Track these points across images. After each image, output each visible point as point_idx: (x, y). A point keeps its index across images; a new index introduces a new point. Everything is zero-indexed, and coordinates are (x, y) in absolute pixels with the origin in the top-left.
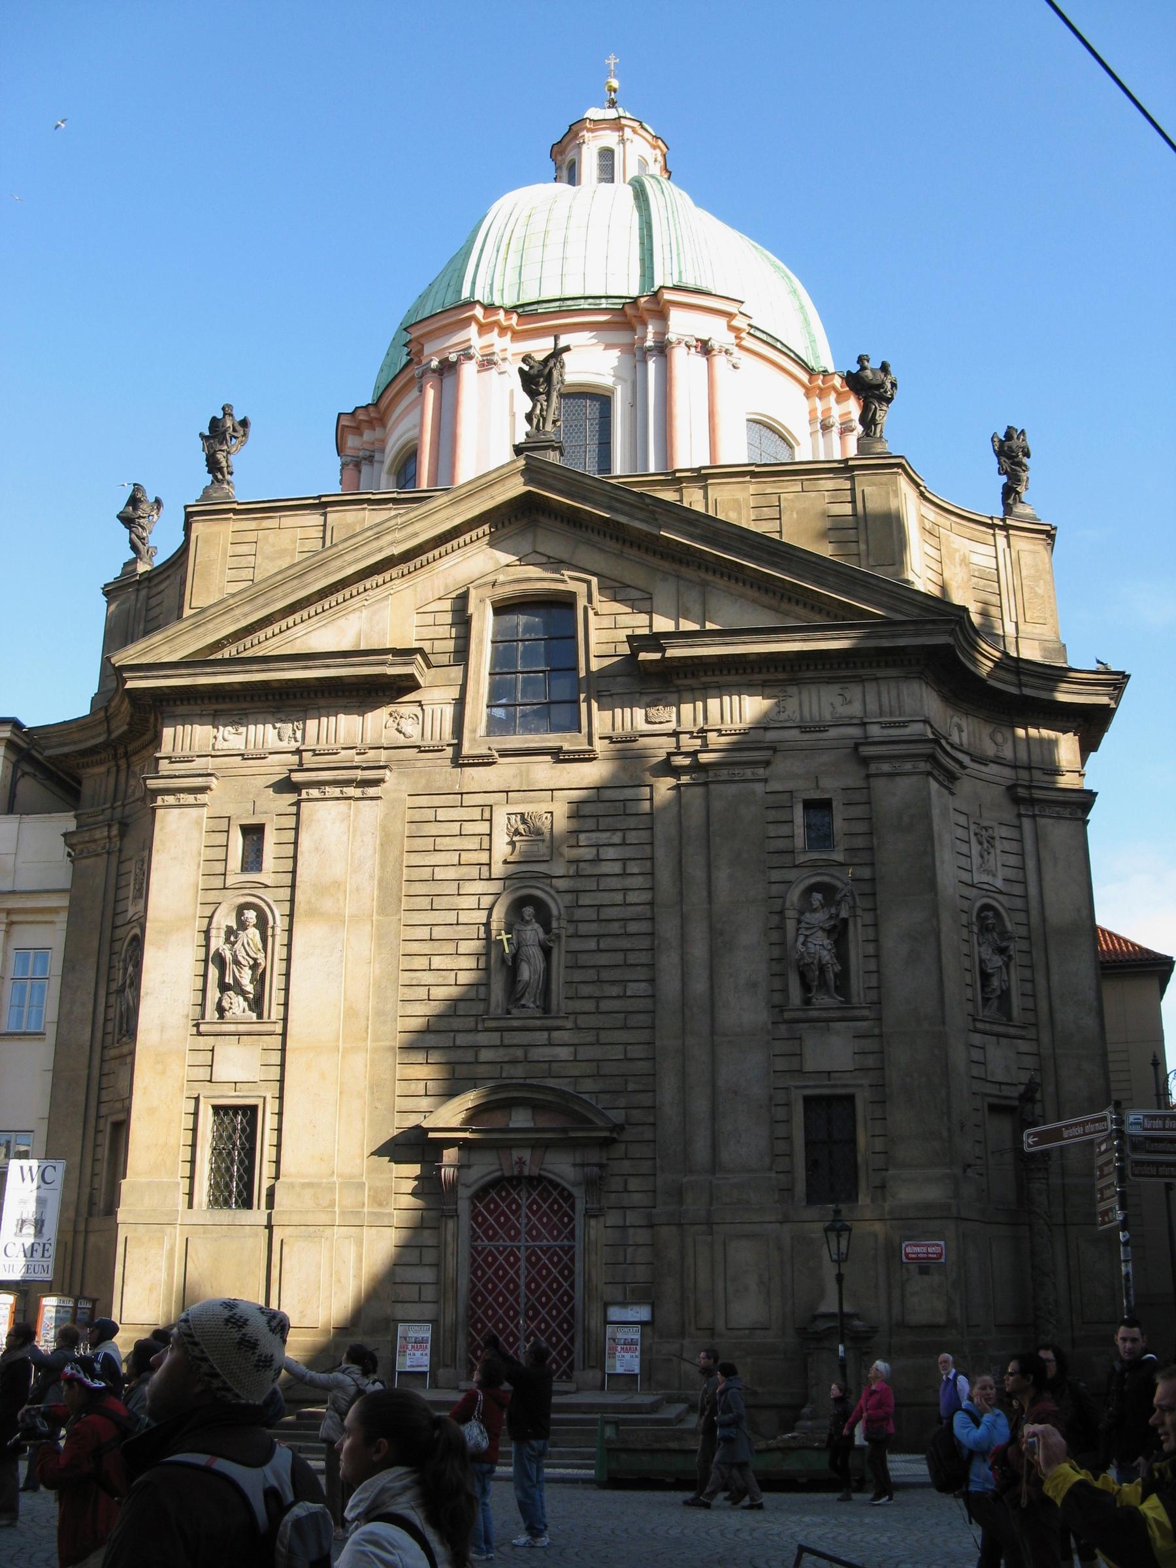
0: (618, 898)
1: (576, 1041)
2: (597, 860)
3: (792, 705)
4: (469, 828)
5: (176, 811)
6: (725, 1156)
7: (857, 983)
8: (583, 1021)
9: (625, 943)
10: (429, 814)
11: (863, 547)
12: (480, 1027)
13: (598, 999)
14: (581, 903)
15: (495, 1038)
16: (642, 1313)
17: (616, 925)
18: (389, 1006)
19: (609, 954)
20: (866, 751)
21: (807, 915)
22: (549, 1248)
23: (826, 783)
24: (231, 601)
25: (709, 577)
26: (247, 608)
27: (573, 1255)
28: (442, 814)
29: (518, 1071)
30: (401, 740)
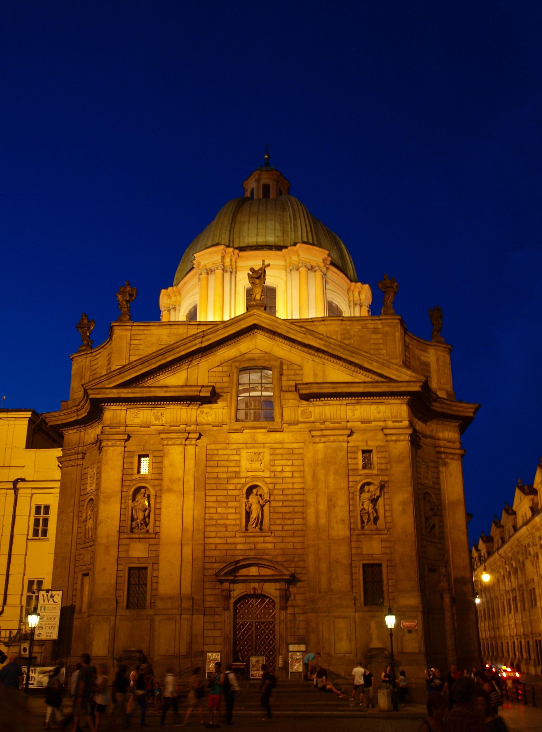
0: (291, 486)
1: (275, 541)
2: (282, 471)
3: (357, 413)
4: (232, 458)
5: (112, 448)
6: (333, 586)
7: (381, 521)
8: (277, 533)
9: (294, 504)
10: (215, 452)
11: (385, 351)
14: (276, 488)
15: (243, 540)
16: (303, 647)
20: (386, 431)
21: (363, 494)
22: (264, 622)
23: (370, 443)
24: (135, 363)
25: (325, 361)
26: (140, 367)
27: (275, 625)
28: (220, 452)
29: (252, 553)
30: (204, 421)
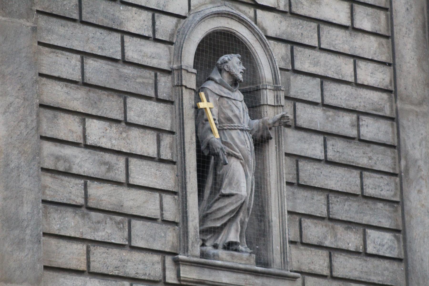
0: (345, 68)
18: (26, 209)
19: (340, 171)
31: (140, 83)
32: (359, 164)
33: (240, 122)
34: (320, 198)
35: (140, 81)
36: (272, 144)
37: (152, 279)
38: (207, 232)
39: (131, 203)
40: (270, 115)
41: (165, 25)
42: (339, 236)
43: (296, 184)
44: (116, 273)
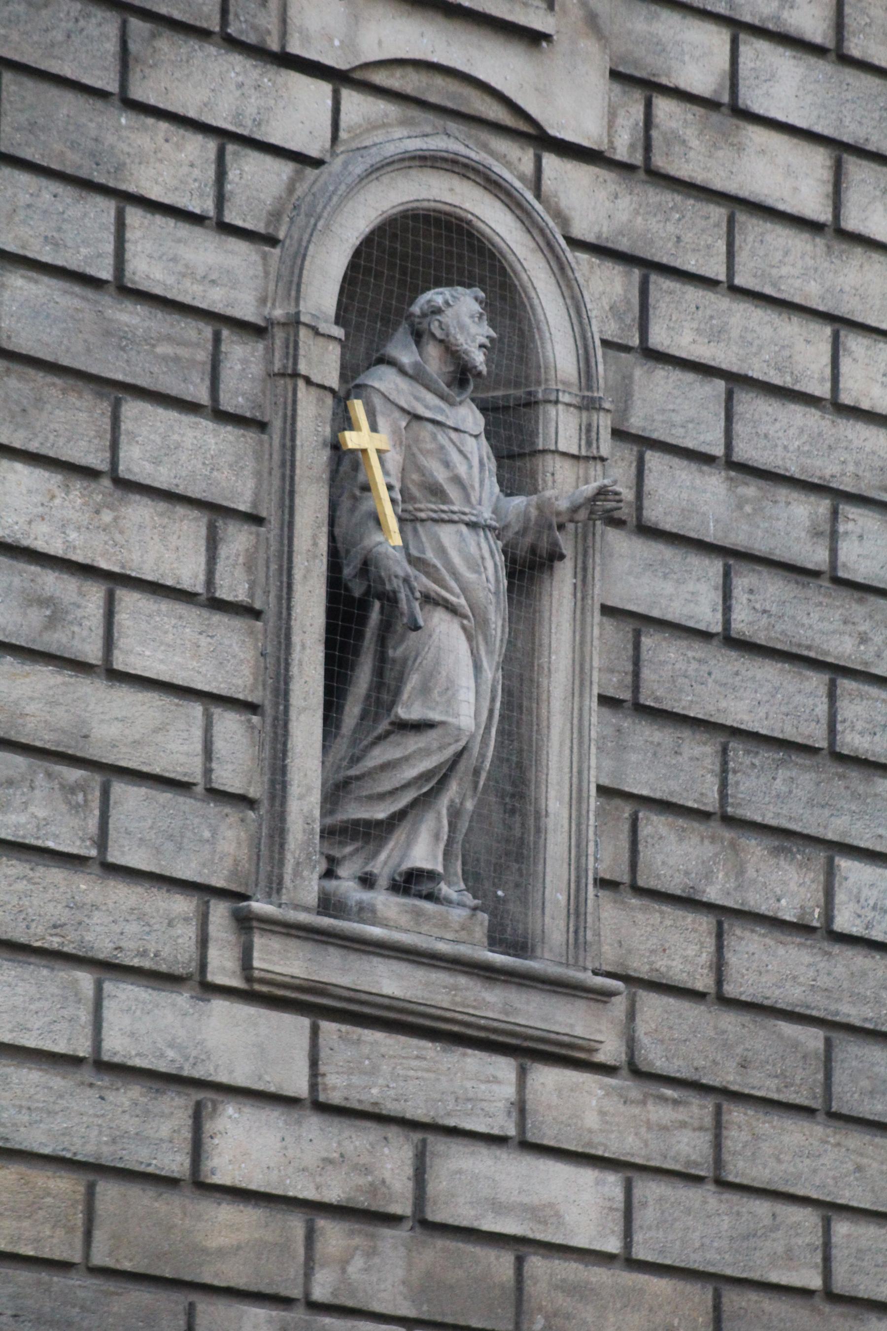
12: (223, 967)
13: (725, 916)
17: (803, 510)
19: (768, 672)
31: (165, 358)
32: (827, 653)
33: (467, 499)
34: (701, 751)
35: (165, 353)
36: (564, 578)
37: (164, 968)
38: (347, 835)
39: (112, 731)
40: (563, 485)
41: (257, 183)
42: (751, 873)
43: (631, 704)
44: (54, 942)
